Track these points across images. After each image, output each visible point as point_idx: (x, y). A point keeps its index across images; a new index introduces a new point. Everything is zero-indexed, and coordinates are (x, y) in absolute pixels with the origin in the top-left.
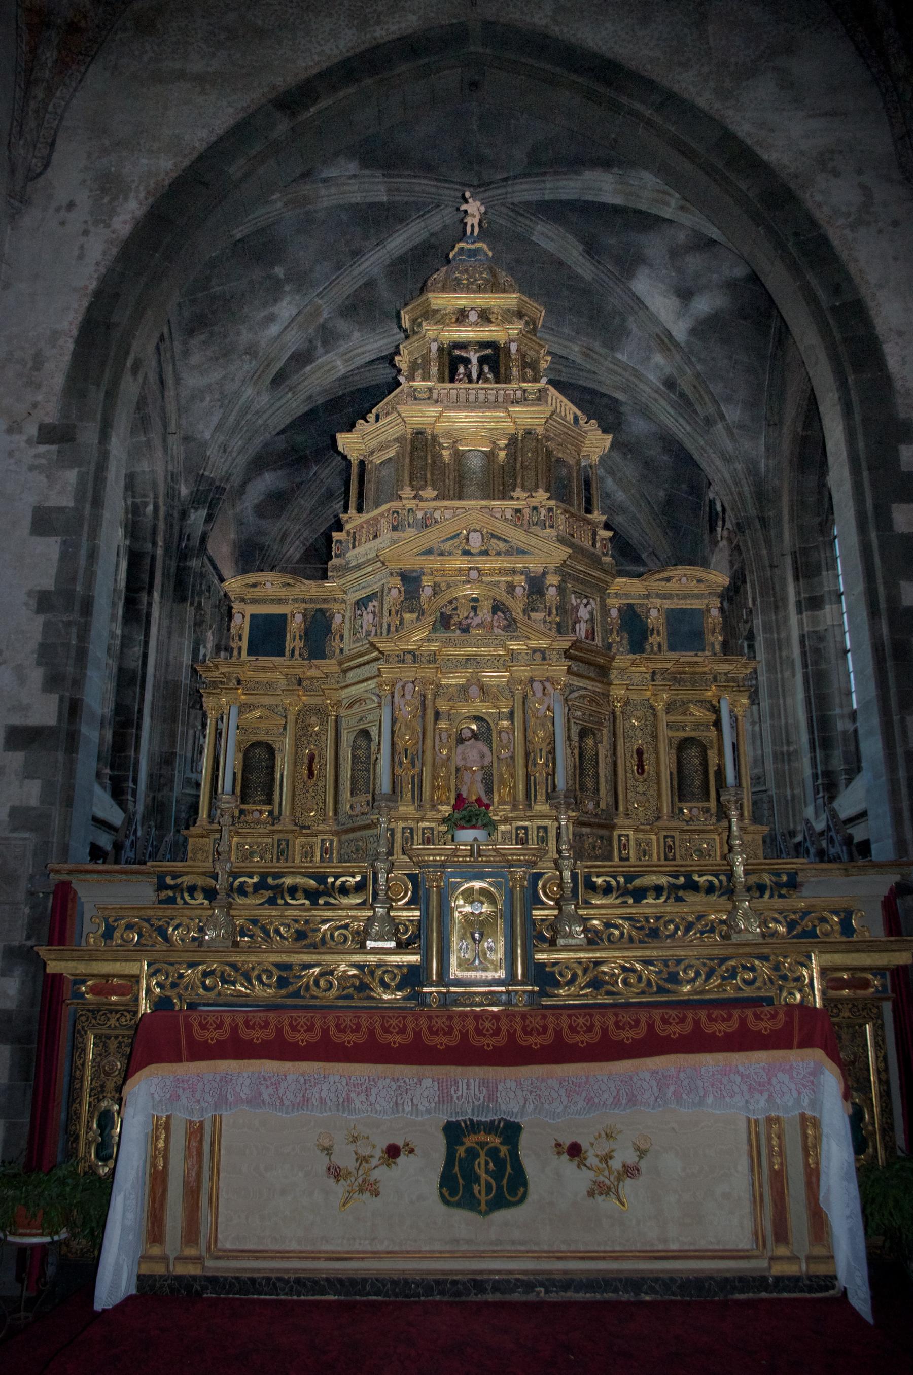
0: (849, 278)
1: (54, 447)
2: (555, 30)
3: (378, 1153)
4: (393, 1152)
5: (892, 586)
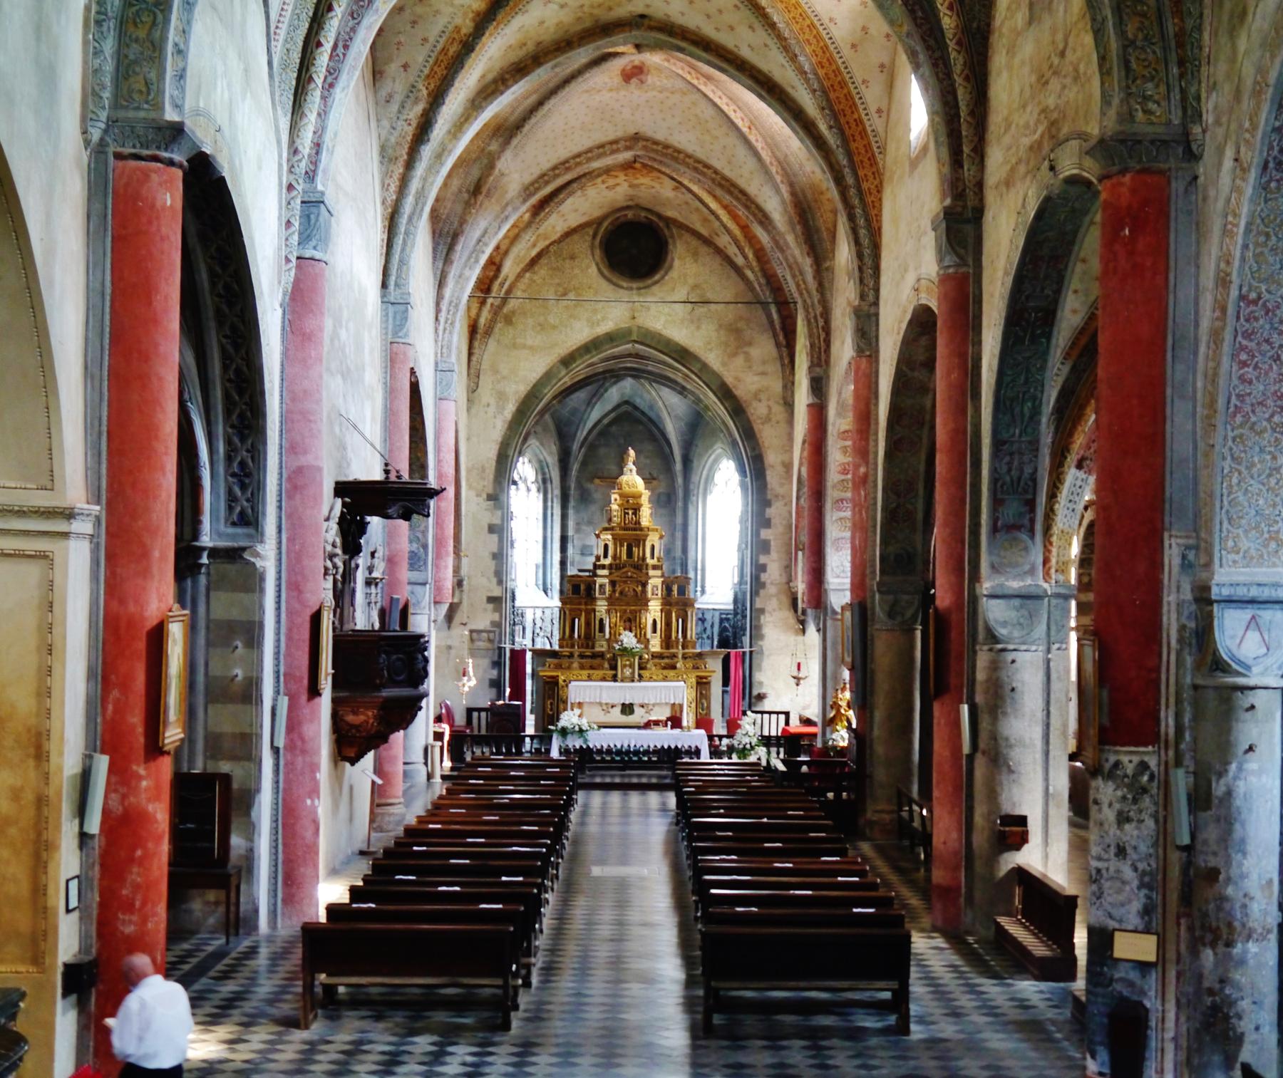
0: (758, 444)
5: (757, 556)
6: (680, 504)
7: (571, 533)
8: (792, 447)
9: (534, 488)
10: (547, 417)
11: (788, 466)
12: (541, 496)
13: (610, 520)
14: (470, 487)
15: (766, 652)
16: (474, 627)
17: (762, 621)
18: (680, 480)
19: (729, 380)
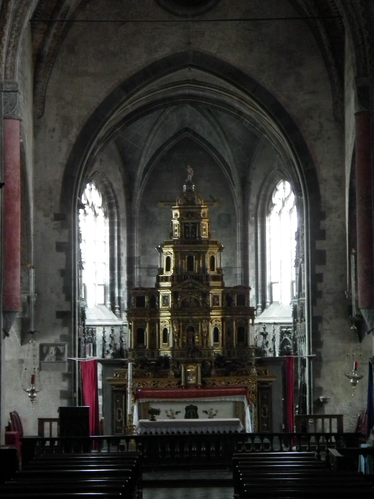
1: (59, 222)
2: (219, 55)
3: (175, 413)
4: (177, 413)
6: (239, 224)
7: (136, 254)
8: (343, 161)
9: (101, 212)
10: (112, 145)
11: (340, 180)
12: (108, 220)
13: (171, 235)
14: (38, 207)
15: (324, 359)
16: (45, 341)
17: (320, 329)
18: (238, 202)
19: (282, 99)
